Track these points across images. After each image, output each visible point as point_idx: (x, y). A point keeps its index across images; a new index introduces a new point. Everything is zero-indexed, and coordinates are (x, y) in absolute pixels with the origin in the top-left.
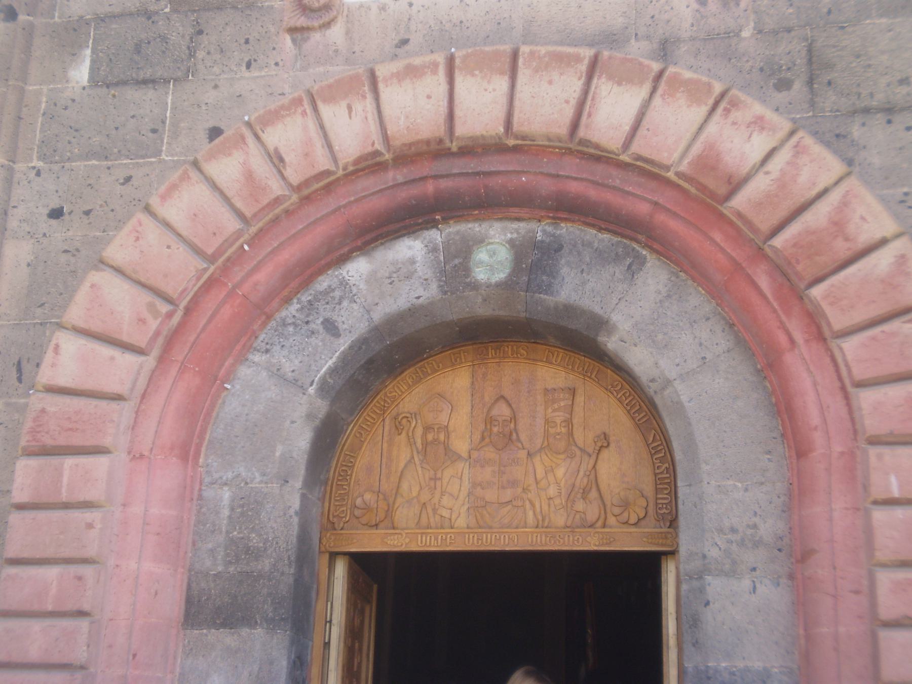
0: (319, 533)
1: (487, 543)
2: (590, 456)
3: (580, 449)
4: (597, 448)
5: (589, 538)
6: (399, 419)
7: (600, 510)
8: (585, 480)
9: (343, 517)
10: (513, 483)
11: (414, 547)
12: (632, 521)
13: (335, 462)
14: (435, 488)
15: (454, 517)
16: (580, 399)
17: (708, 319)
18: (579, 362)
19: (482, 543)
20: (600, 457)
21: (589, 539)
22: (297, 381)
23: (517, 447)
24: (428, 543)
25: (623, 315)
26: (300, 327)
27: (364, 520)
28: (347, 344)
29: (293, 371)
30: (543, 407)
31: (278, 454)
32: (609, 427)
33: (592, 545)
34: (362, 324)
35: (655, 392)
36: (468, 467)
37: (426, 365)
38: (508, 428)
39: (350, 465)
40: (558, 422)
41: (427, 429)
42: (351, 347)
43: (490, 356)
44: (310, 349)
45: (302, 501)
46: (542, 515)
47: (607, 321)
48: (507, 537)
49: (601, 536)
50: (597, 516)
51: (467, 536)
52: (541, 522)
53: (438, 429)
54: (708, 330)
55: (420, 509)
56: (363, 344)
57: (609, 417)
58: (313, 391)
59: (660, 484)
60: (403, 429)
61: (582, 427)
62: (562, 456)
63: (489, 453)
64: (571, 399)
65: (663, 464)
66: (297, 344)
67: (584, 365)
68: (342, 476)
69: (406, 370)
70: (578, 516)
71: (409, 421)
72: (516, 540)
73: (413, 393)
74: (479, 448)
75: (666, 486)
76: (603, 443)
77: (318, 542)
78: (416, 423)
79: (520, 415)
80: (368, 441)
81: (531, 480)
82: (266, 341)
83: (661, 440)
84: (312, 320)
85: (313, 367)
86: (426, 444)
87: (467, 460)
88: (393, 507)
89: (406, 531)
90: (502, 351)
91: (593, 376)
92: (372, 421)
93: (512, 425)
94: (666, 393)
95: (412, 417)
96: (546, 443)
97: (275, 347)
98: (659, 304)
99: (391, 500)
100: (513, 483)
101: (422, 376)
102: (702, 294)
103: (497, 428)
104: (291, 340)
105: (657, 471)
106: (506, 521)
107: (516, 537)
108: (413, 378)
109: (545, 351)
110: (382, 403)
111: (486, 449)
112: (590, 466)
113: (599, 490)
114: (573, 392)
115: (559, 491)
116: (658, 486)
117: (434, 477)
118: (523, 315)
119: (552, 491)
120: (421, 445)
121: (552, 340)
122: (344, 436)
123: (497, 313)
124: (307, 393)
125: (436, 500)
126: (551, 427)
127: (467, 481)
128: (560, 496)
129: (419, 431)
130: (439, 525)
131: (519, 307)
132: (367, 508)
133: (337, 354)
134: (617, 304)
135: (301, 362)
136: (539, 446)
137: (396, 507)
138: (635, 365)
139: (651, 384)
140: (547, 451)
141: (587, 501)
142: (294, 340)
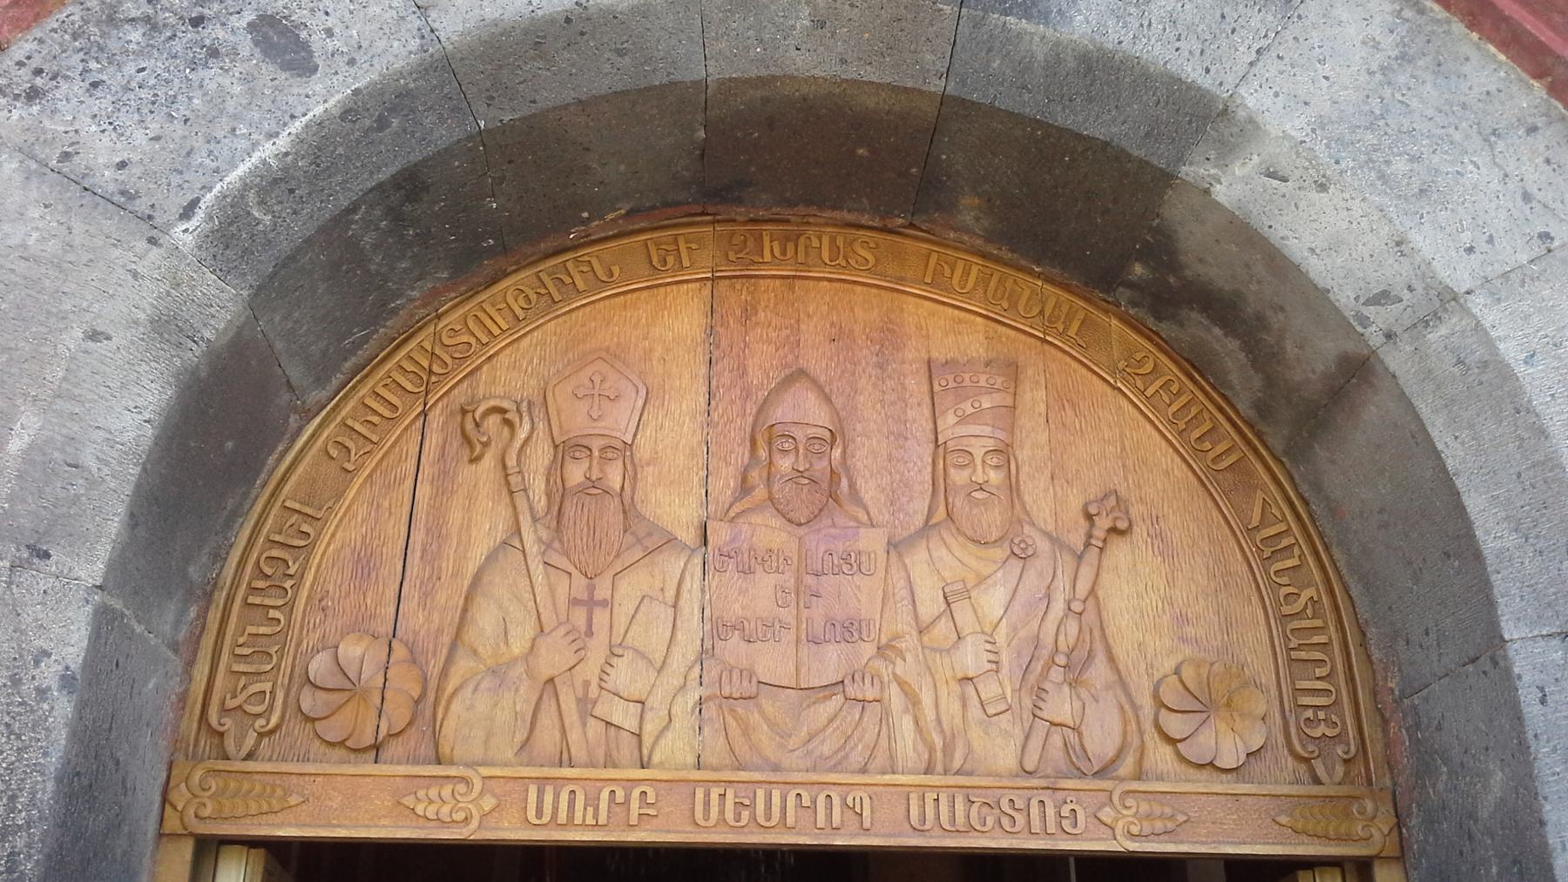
0: (165, 767)
1: (768, 817)
2: (1080, 558)
3: (1047, 535)
4: (1099, 533)
5: (1107, 809)
6: (477, 415)
7: (1125, 723)
8: (1072, 627)
9: (258, 716)
10: (849, 629)
11: (511, 830)
12: (1228, 761)
13: (247, 532)
14: (590, 632)
15: (650, 729)
16: (1034, 398)
17: (1533, 130)
18: (1027, 293)
19: (754, 818)
20: (1105, 563)
21: (1107, 814)
22: (132, 198)
23: (857, 520)
24: (562, 817)
25: (1276, 95)
26: (168, 34)
27: (331, 730)
28: (338, 97)
29: (122, 165)
30: (927, 412)
31: (15, 445)
32: (1126, 479)
33: (1118, 832)
34: (396, 44)
35: (1389, 336)
36: (699, 569)
37: (570, 265)
38: (825, 463)
39: (302, 543)
40: (978, 454)
41: (565, 450)
42: (348, 113)
43: (767, 256)
44: (196, 101)
45: (96, 636)
46: (942, 731)
47: (1225, 110)
48: (836, 801)
49: (1144, 807)
50: (1118, 740)
51: (700, 794)
52: (939, 755)
53: (603, 449)
54: (1539, 160)
55: (534, 698)
56: (392, 110)
57: (1123, 448)
58: (189, 238)
59: (1299, 648)
60: (486, 445)
61: (1047, 473)
62: (999, 553)
63: (768, 531)
64: (1012, 390)
65: (1303, 587)
66: (152, 82)
67: (1043, 303)
68: (267, 577)
69: (506, 275)
70: (1056, 740)
71: (508, 423)
72: (866, 813)
73: (525, 343)
74: (731, 513)
75: (1318, 655)
76: (1116, 519)
77: (158, 798)
78: (533, 429)
79: (859, 427)
80: (367, 472)
81: (902, 622)
82: (35, 63)
83: (1284, 519)
84: (217, 17)
85: (197, 159)
86: (559, 495)
87: (693, 550)
88: (440, 689)
89: (485, 771)
90: (801, 248)
91: (1072, 332)
92: (387, 414)
93: (837, 453)
94: (1436, 336)
95: (518, 410)
96: (941, 513)
97: (64, 86)
98: (1379, 76)
99: (434, 668)
100: (849, 629)
101: (557, 297)
102: (1500, 63)
103: (792, 457)
104: (130, 69)
105: (1287, 610)
106: (826, 749)
107: (866, 801)
108: (529, 301)
109: (929, 256)
110: (425, 364)
111: (757, 519)
112: (1083, 587)
113: (1111, 659)
114: (1013, 371)
115: (992, 657)
116: (1294, 655)
117: (585, 597)
118: (936, 85)
119: (971, 658)
120: (544, 498)
121: (969, 209)
122: (287, 450)
123: (851, 73)
124: (164, 240)
125: (591, 670)
126: (955, 466)
127: (697, 612)
128: (997, 672)
129: (540, 456)
130: (600, 754)
131: (928, 56)
132: (348, 688)
133: (297, 126)
134: (1251, 64)
135: (157, 138)
136: (919, 521)
137: (450, 689)
138: (1312, 250)
139: (1370, 311)
140: (945, 534)
141: (1084, 693)
142: (143, 69)
